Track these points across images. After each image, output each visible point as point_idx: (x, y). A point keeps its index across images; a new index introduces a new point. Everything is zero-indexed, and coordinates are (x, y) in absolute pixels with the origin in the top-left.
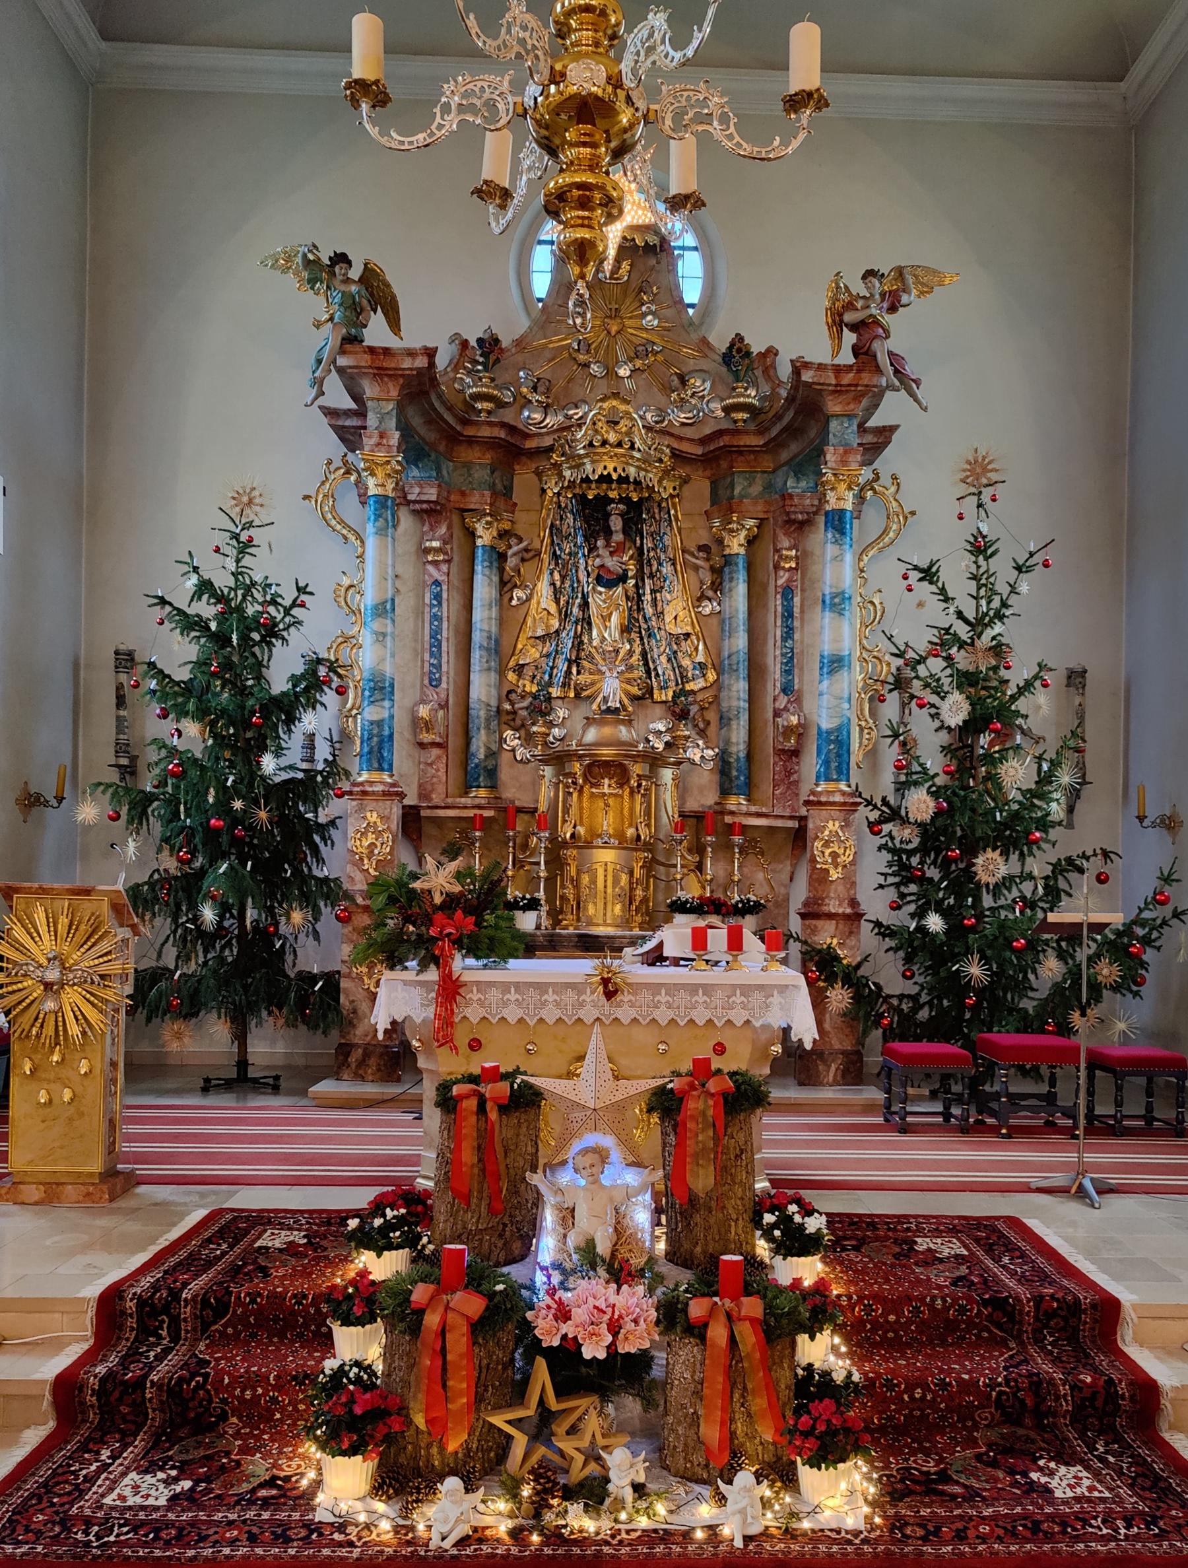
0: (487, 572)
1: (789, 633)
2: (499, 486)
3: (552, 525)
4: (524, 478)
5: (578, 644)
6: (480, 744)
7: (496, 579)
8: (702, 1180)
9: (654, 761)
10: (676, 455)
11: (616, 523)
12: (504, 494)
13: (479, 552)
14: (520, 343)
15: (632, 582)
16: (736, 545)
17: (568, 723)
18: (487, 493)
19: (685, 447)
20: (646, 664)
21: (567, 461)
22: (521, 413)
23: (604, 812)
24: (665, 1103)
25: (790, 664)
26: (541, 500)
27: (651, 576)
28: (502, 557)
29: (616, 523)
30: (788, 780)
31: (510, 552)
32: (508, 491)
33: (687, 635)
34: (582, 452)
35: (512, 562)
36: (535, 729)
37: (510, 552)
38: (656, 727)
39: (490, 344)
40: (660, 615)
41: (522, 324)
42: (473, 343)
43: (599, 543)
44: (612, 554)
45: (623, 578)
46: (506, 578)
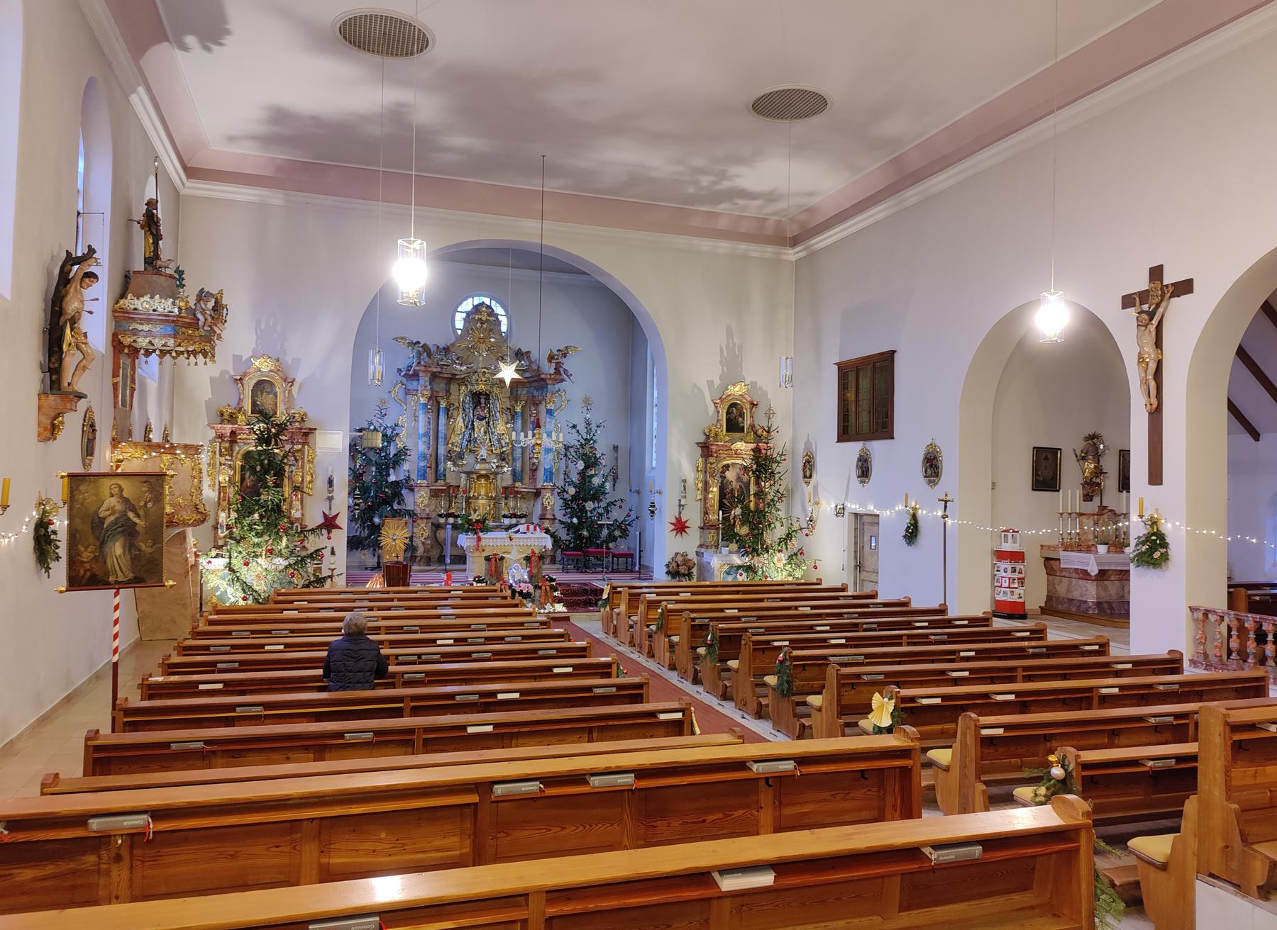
4: (454, 387)
6: (441, 467)
8: (535, 571)
9: (496, 474)
12: (448, 392)
14: (453, 345)
16: (518, 409)
23: (482, 488)
24: (528, 559)
26: (461, 394)
30: (533, 478)
38: (494, 462)
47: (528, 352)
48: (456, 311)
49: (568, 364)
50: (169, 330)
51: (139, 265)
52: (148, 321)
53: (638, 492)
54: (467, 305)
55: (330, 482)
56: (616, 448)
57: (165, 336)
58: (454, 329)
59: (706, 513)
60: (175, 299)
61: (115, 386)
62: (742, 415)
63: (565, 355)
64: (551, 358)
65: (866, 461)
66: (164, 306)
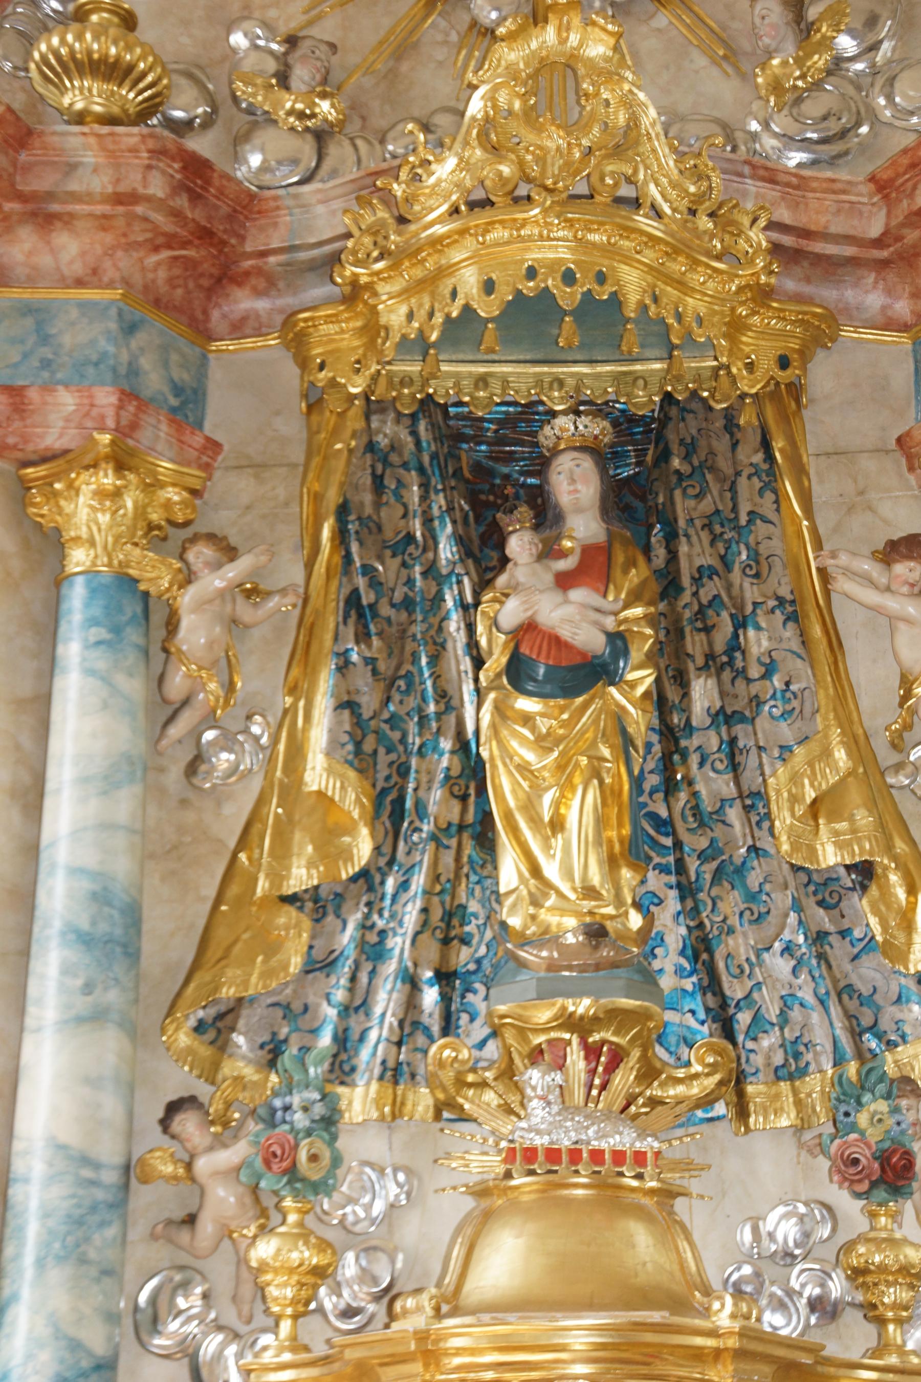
0: (101, 660)
2: (153, 381)
3: (343, 511)
5: (446, 924)
7: (134, 686)
10: (793, 250)
11: (576, 486)
13: (77, 596)
15: (643, 678)
17: (410, 1231)
18: (106, 398)
19: (820, 214)
20: (712, 985)
21: (395, 266)
22: (238, 158)
27: (712, 664)
29: (576, 486)
31: (186, 599)
32: (187, 406)
33: (865, 872)
34: (439, 230)
35: (195, 633)
36: (264, 1250)
37: (186, 599)
40: (754, 802)
43: (520, 545)
44: (564, 582)
46: (177, 684)
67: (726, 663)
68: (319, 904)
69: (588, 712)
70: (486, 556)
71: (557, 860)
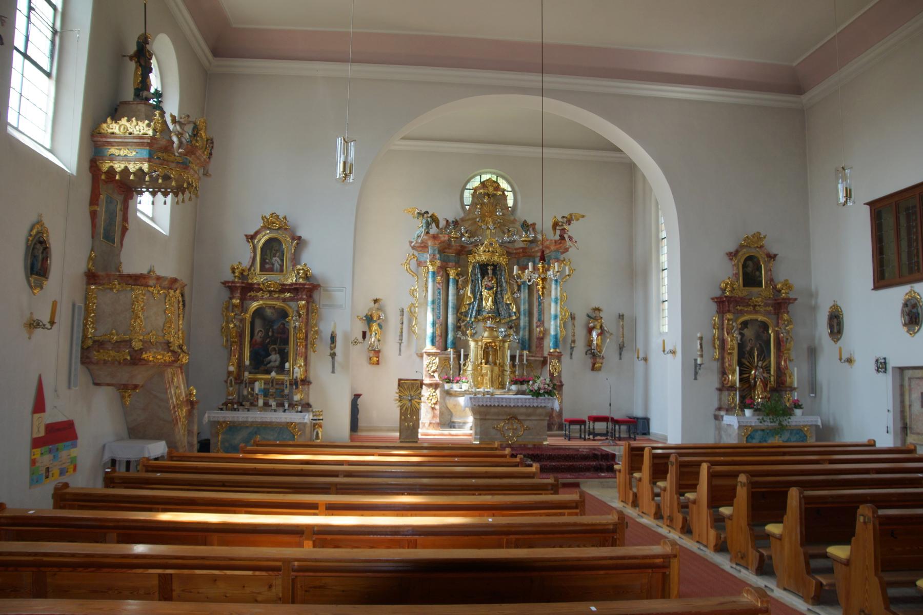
1: (540, 304)
11: (490, 272)
25: (541, 312)
28: (457, 281)
29: (490, 272)
35: (460, 282)
39: (456, 223)
41: (462, 215)
42: (450, 221)
45: (492, 288)
47: (534, 224)
48: (464, 188)
49: (572, 230)
50: (145, 153)
51: (129, 95)
52: (125, 144)
53: (645, 359)
54: (476, 182)
55: (333, 339)
56: (621, 317)
57: (141, 160)
58: (463, 206)
59: (723, 373)
60: (151, 121)
61: (94, 215)
62: (759, 269)
63: (569, 222)
64: (555, 225)
65: (915, 306)
66: (141, 128)
67: (501, 286)
68: (469, 304)
69: (491, 292)
70: (483, 278)
71: (488, 304)
